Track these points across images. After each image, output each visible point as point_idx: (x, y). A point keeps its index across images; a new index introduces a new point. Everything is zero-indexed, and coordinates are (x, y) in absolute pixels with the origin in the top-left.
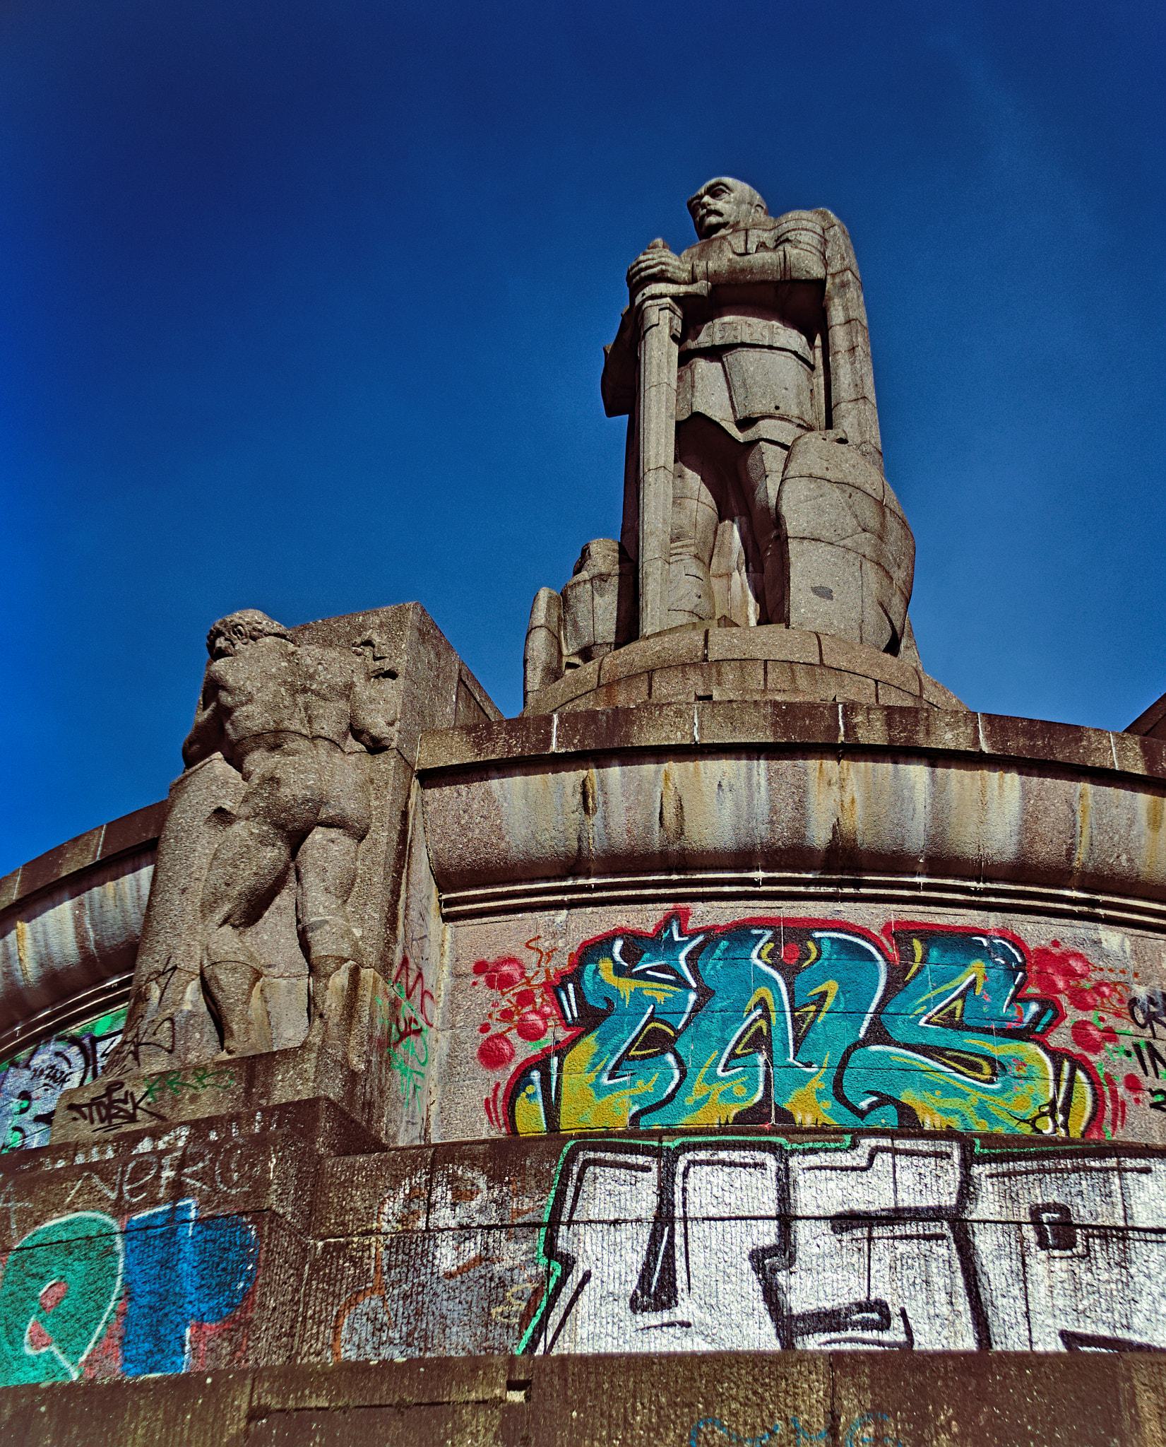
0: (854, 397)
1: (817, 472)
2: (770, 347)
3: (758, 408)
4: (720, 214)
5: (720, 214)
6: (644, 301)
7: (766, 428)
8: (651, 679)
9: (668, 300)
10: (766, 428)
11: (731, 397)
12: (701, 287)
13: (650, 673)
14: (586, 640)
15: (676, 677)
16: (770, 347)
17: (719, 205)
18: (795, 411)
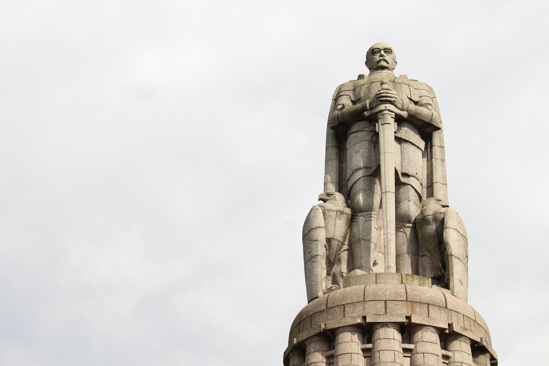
0: (443, 183)
1: (458, 230)
2: (418, 147)
3: (411, 172)
4: (388, 63)
5: (388, 63)
6: (385, 110)
7: (411, 181)
8: (428, 307)
9: (394, 114)
10: (411, 181)
11: (402, 161)
12: (405, 114)
13: (428, 304)
14: (330, 236)
15: (436, 308)
16: (418, 147)
17: (387, 57)
18: (420, 178)
